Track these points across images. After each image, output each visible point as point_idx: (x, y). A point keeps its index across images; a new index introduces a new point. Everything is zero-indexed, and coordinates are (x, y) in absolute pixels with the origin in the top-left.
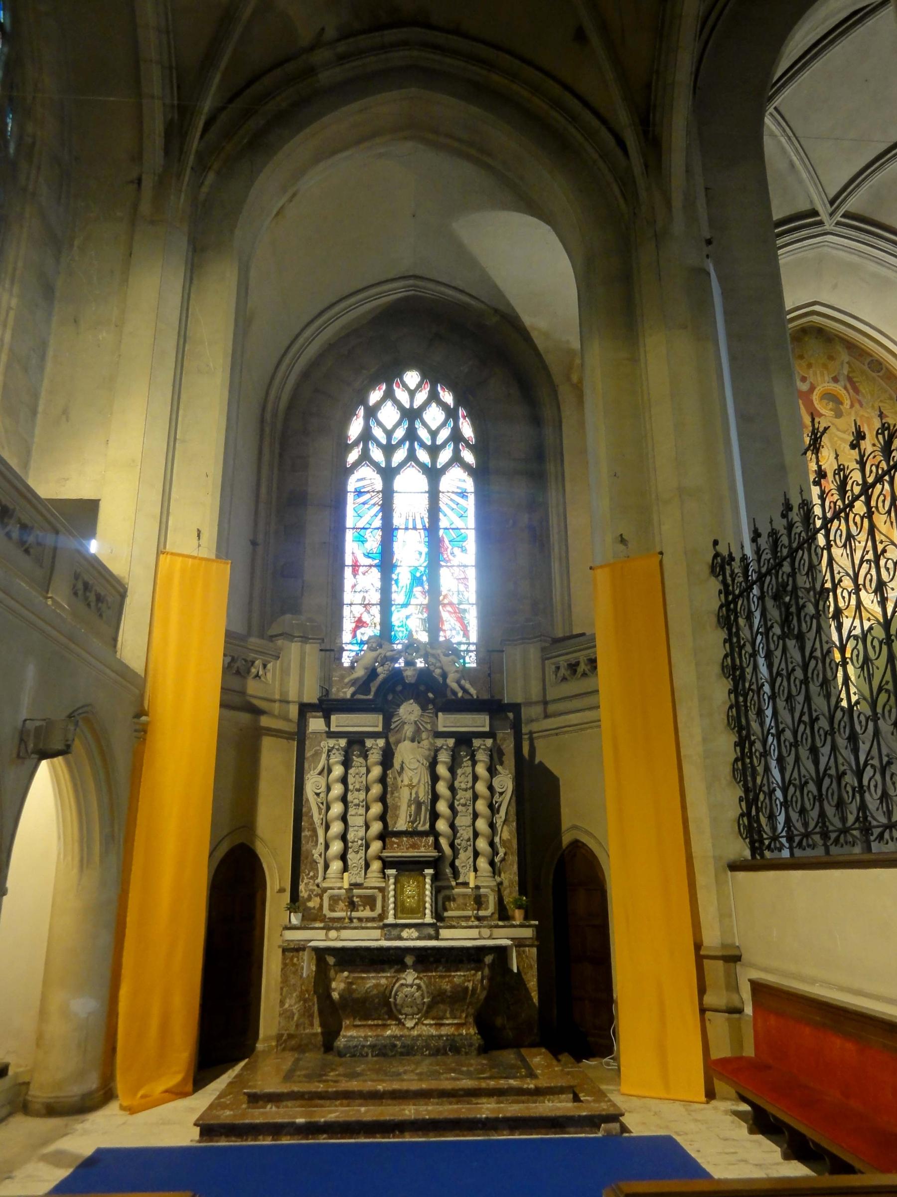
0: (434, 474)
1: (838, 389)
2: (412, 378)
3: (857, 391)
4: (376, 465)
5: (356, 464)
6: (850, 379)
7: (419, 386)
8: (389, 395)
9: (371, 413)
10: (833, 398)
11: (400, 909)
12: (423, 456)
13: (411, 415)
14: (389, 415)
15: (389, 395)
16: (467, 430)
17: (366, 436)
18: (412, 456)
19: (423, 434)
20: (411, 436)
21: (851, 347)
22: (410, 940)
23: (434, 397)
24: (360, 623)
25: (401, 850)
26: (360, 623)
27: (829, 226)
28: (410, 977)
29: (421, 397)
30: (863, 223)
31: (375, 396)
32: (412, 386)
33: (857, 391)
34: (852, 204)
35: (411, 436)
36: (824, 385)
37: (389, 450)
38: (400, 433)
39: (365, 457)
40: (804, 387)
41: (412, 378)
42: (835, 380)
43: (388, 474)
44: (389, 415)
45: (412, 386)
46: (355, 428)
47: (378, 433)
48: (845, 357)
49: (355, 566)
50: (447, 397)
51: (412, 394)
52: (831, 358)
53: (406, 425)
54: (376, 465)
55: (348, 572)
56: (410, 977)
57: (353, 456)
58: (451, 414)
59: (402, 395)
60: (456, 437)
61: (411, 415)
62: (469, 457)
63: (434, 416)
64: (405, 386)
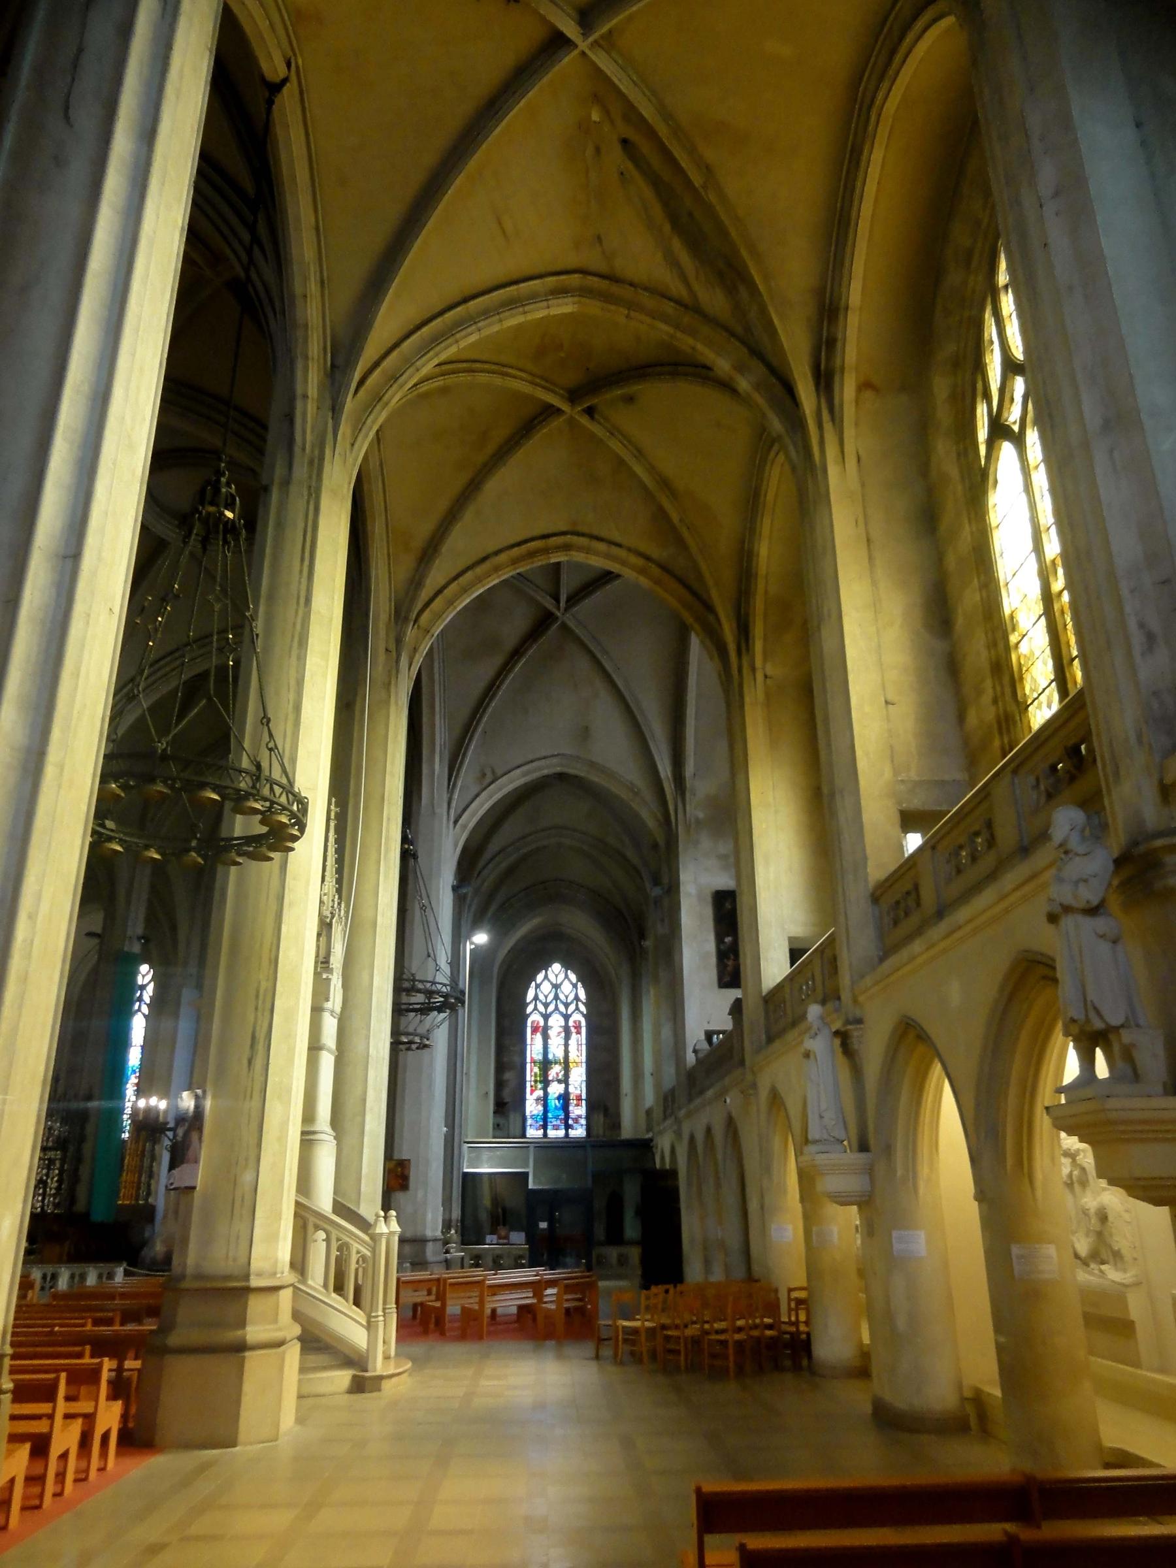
2: (556, 967)
4: (541, 1013)
8: (546, 977)
9: (538, 986)
12: (562, 1008)
13: (556, 987)
14: (546, 987)
16: (582, 994)
17: (536, 998)
18: (557, 1008)
19: (562, 997)
20: (556, 997)
23: (566, 976)
29: (562, 976)
35: (556, 997)
37: (546, 1005)
39: (536, 1008)
41: (556, 967)
43: (546, 1017)
44: (546, 987)
47: (541, 997)
50: (573, 977)
57: (529, 1009)
58: (575, 986)
59: (551, 976)
61: (556, 987)
63: (567, 988)
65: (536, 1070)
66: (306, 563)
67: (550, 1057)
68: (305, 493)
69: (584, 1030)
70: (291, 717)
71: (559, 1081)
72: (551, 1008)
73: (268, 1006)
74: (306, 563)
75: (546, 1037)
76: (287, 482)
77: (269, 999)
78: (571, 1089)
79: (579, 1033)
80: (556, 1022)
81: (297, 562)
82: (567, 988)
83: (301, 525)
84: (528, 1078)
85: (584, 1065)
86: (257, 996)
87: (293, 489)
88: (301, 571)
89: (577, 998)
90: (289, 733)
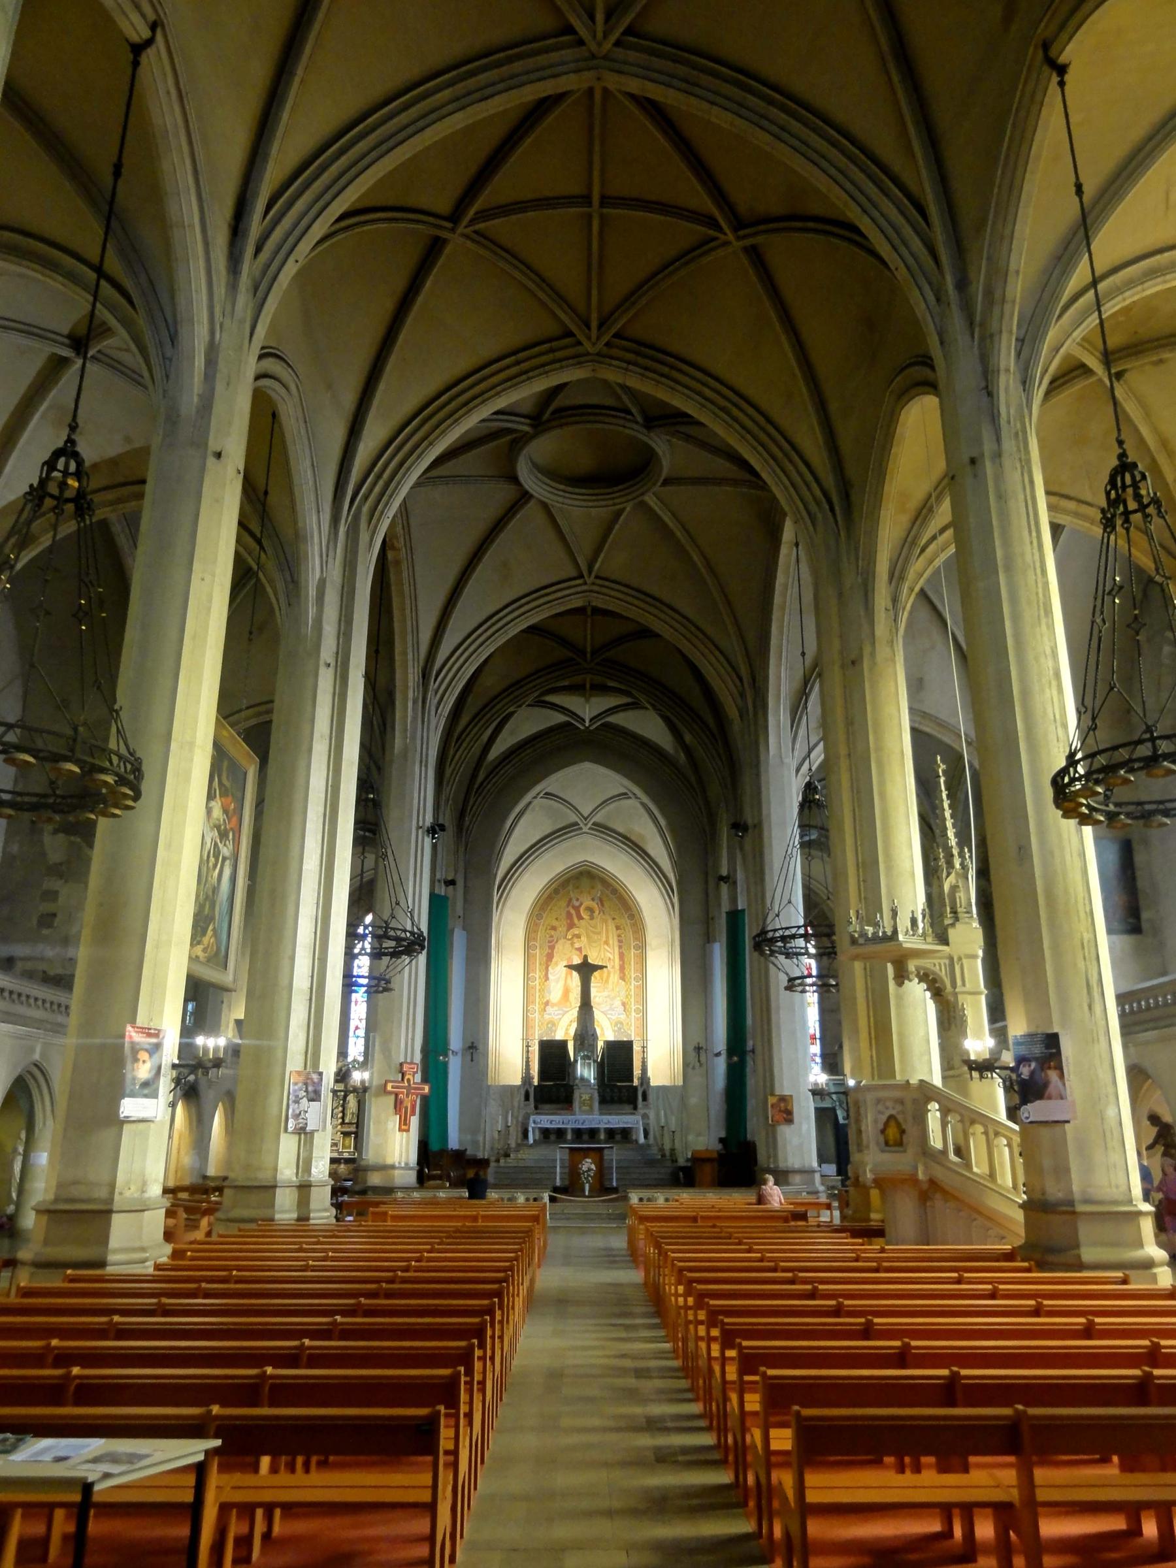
1: (594, 905)
3: (603, 905)
6: (601, 900)
10: (590, 910)
11: (344, 1147)
21: (604, 882)
22: (346, 1155)
24: (357, 1028)
25: (347, 1129)
26: (357, 1028)
27: (585, 829)
28: (342, 1166)
30: (602, 829)
33: (603, 905)
34: (598, 818)
36: (587, 902)
40: (577, 904)
42: (593, 900)
48: (599, 886)
49: (356, 1002)
52: (593, 888)
55: (353, 1004)
56: (342, 1166)
66: (1034, 534)
68: (1018, 465)
70: (1054, 683)
73: (1094, 956)
74: (1034, 534)
76: (998, 455)
77: (1093, 950)
81: (1026, 533)
83: (1021, 497)
86: (1083, 948)
87: (1007, 462)
88: (1031, 543)
90: (1055, 699)
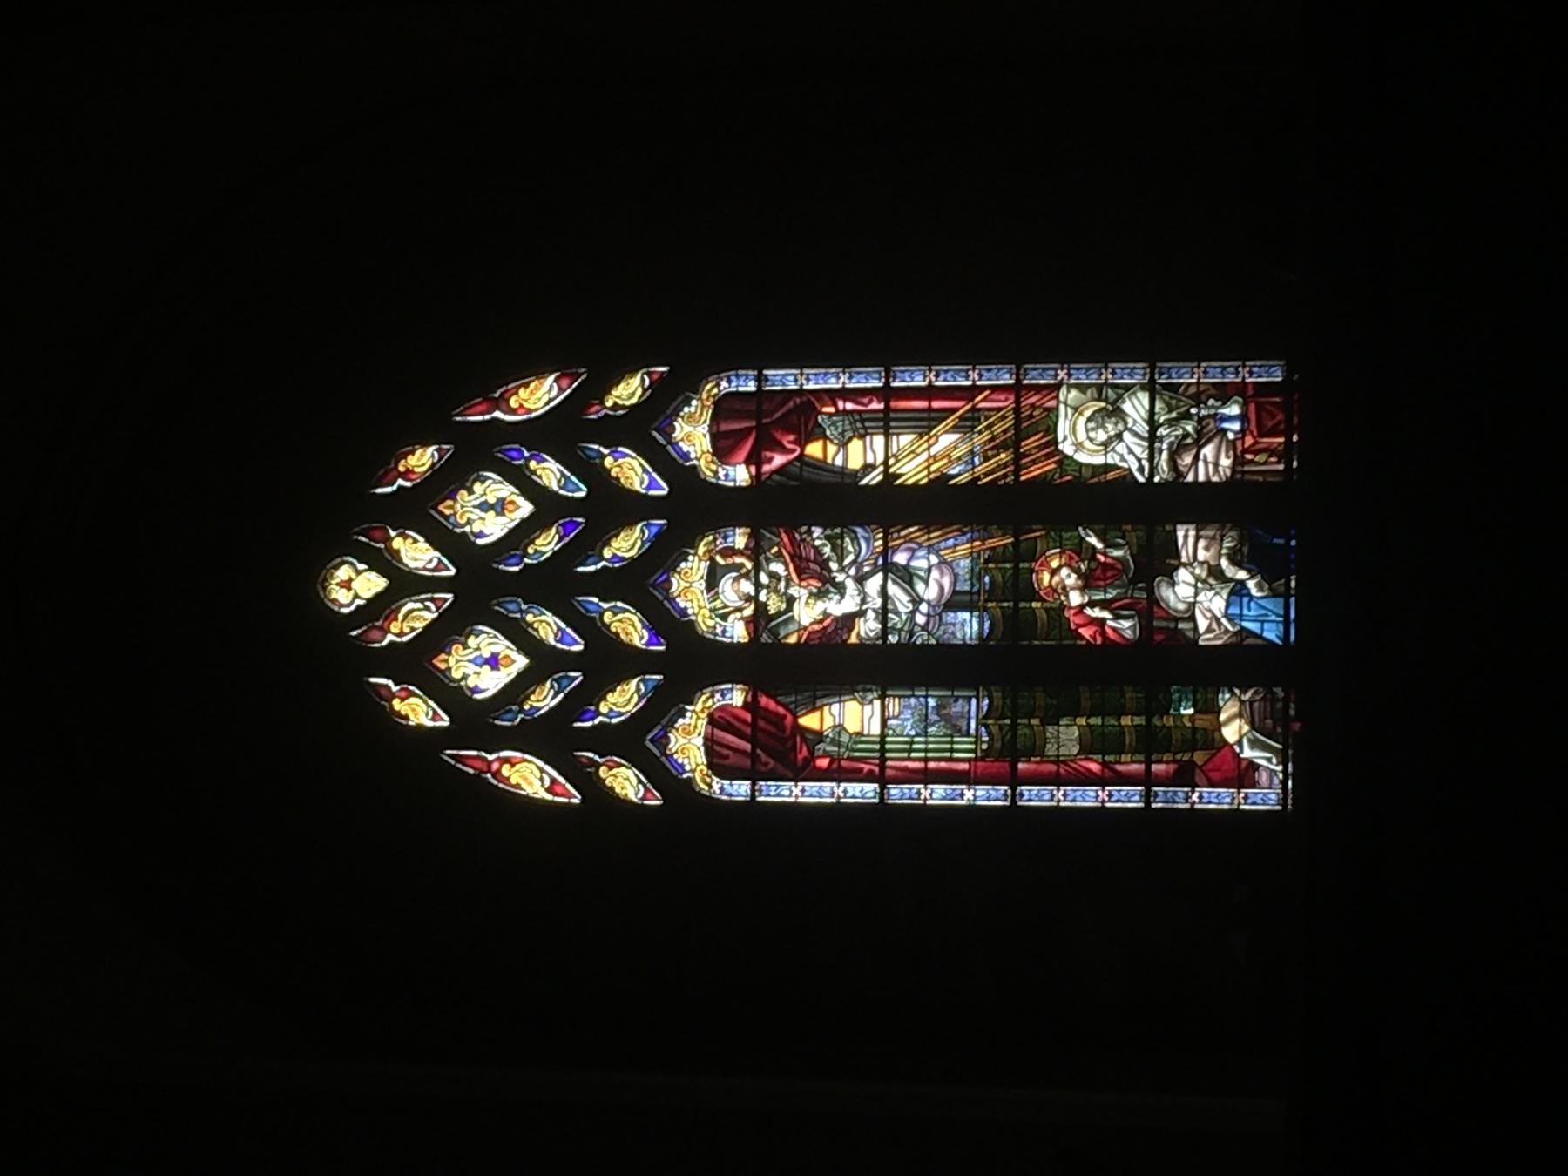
0: (691, 510)
5: (659, 771)
7: (384, 562)
9: (476, 721)
13: (482, 587)
14: (483, 664)
15: (417, 663)
17: (552, 739)
31: (418, 711)
32: (371, 584)
35: (555, 585)
37: (606, 661)
38: (547, 626)
41: (351, 586)
43: (687, 661)
44: (483, 664)
45: (371, 584)
46: (529, 777)
51: (404, 584)
53: (512, 607)
54: (661, 710)
57: (625, 782)
58: (476, 453)
60: (554, 433)
61: (482, 587)
62: (629, 391)
63: (488, 510)
64: (379, 609)
65: (1067, 737)
67: (967, 626)
69: (783, 379)
71: (1159, 561)
72: (630, 627)
75: (836, 663)
78: (1212, 464)
79: (801, 415)
80: (713, 596)
82: (488, 510)
84: (1127, 797)
85: (1036, 377)
89: (560, 432)
